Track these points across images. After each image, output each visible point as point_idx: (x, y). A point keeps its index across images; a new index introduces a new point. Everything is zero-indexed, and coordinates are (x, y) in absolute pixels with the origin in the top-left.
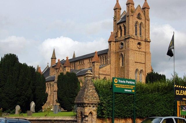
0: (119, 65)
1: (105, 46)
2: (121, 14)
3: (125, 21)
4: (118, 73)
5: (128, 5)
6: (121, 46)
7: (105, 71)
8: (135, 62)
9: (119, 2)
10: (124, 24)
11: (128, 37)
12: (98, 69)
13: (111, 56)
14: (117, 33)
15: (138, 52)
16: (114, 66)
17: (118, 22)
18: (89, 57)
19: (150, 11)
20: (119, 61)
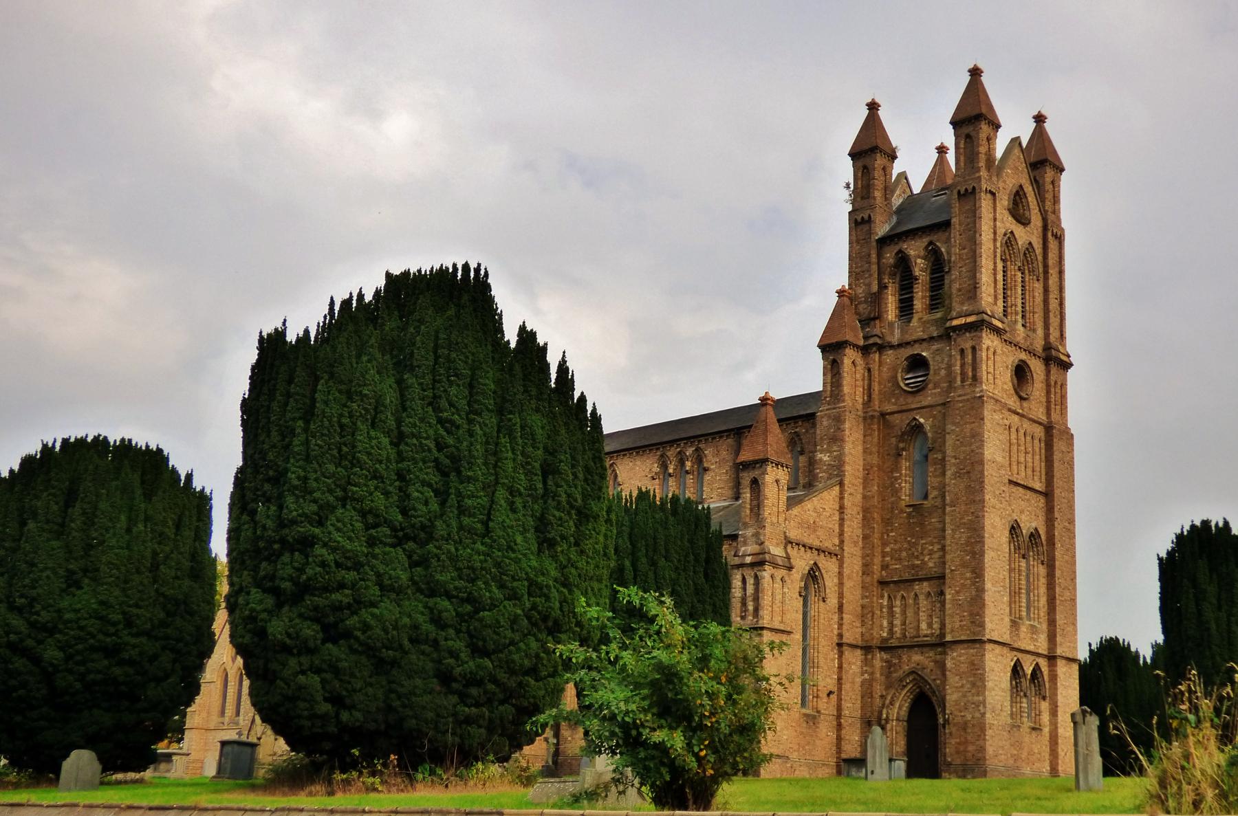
0: (896, 492)
1: (808, 377)
2: (999, 153)
3: (946, 225)
4: (884, 544)
5: (966, 130)
6: (906, 380)
7: (813, 528)
8: (1011, 482)
9: (985, 79)
10: (931, 243)
11: (970, 319)
12: (783, 506)
13: (847, 432)
14: (876, 299)
15: (1016, 418)
16: (859, 497)
17: (882, 228)
18: (733, 427)
19: (1065, 180)
20: (896, 467)
